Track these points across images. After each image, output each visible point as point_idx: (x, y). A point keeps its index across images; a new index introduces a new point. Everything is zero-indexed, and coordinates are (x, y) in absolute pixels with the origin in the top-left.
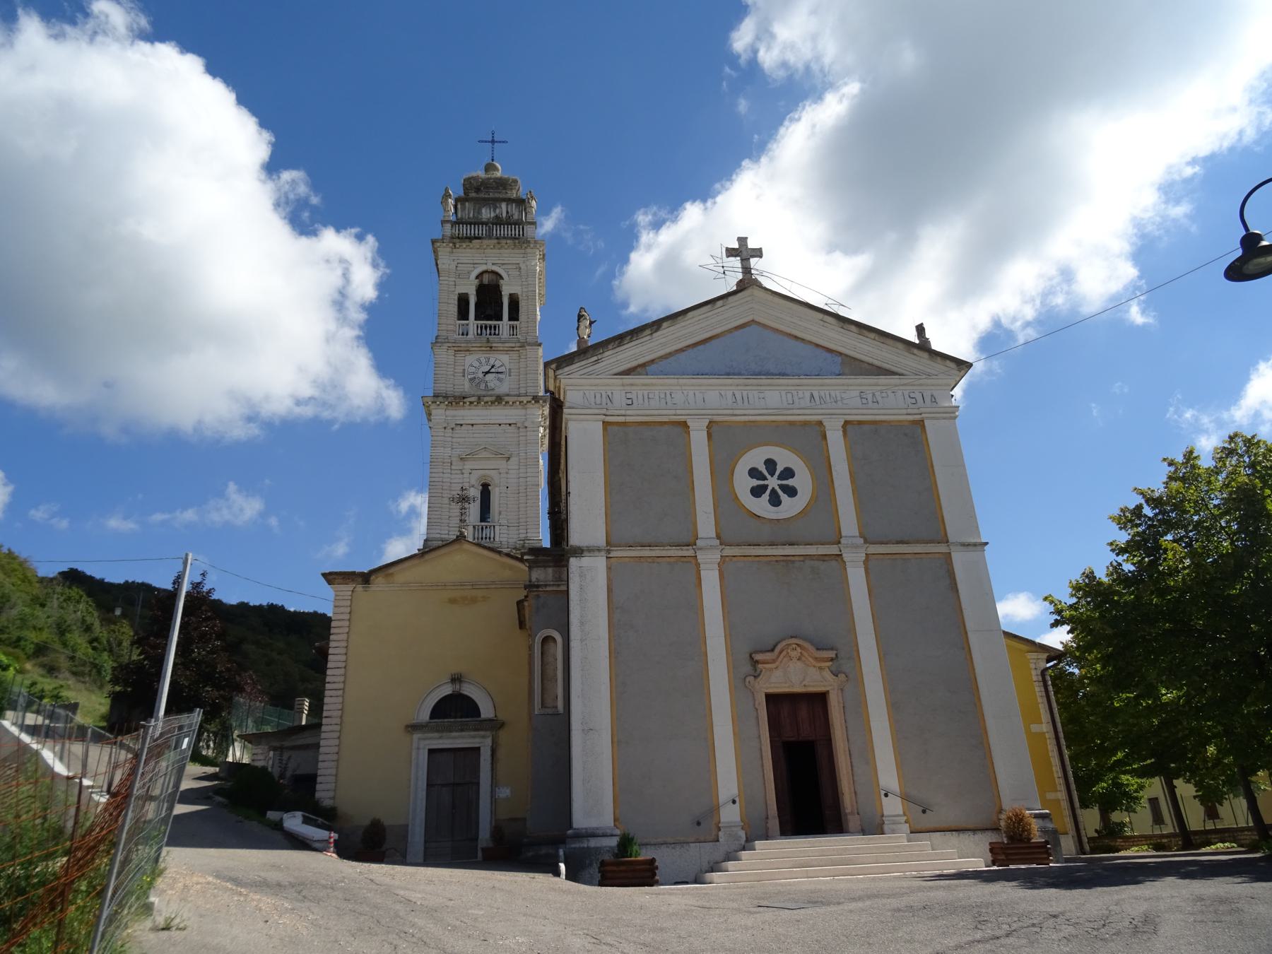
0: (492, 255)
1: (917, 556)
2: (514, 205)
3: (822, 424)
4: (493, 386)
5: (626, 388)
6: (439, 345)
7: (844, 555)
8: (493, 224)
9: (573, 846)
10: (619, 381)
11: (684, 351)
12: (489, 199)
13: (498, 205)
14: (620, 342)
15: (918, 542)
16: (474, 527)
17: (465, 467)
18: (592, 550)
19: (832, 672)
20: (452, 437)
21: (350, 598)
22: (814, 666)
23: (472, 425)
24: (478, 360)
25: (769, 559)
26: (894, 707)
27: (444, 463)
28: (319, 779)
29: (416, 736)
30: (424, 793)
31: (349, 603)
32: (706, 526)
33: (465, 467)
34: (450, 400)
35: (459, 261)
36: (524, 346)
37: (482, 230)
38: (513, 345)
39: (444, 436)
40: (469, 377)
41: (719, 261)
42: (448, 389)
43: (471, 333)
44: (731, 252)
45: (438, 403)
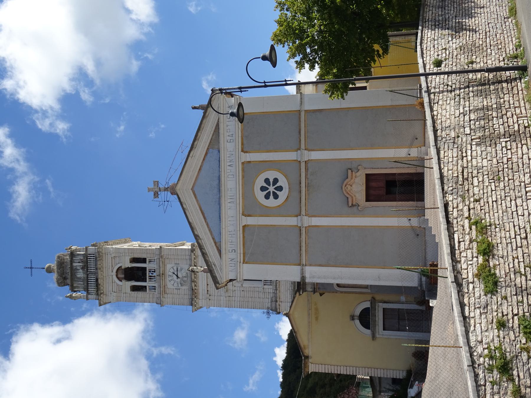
0: (107, 272)
1: (306, 125)
2: (74, 258)
3: (243, 162)
4: (185, 273)
5: (227, 252)
6: (162, 302)
7: (306, 160)
8: (88, 271)
9: (424, 287)
10: (224, 255)
11: (208, 223)
12: (71, 273)
13: (75, 268)
14: (205, 254)
15: (300, 125)
16: (264, 285)
17: (231, 289)
18: (302, 272)
19: (357, 172)
20: (215, 296)
21: (315, 365)
22: (355, 179)
23: (208, 285)
24: (170, 281)
25: (307, 194)
26: (372, 146)
27: (229, 301)
28: (395, 377)
29: (377, 336)
30: (402, 332)
31: (317, 365)
32: (292, 221)
33: (231, 289)
34: (194, 297)
35: (111, 291)
36: (162, 256)
37: (92, 278)
38: (161, 262)
39: (214, 300)
40: (180, 286)
41: (161, 203)
42: (187, 298)
43: (154, 285)
44: (156, 195)
45: (196, 303)
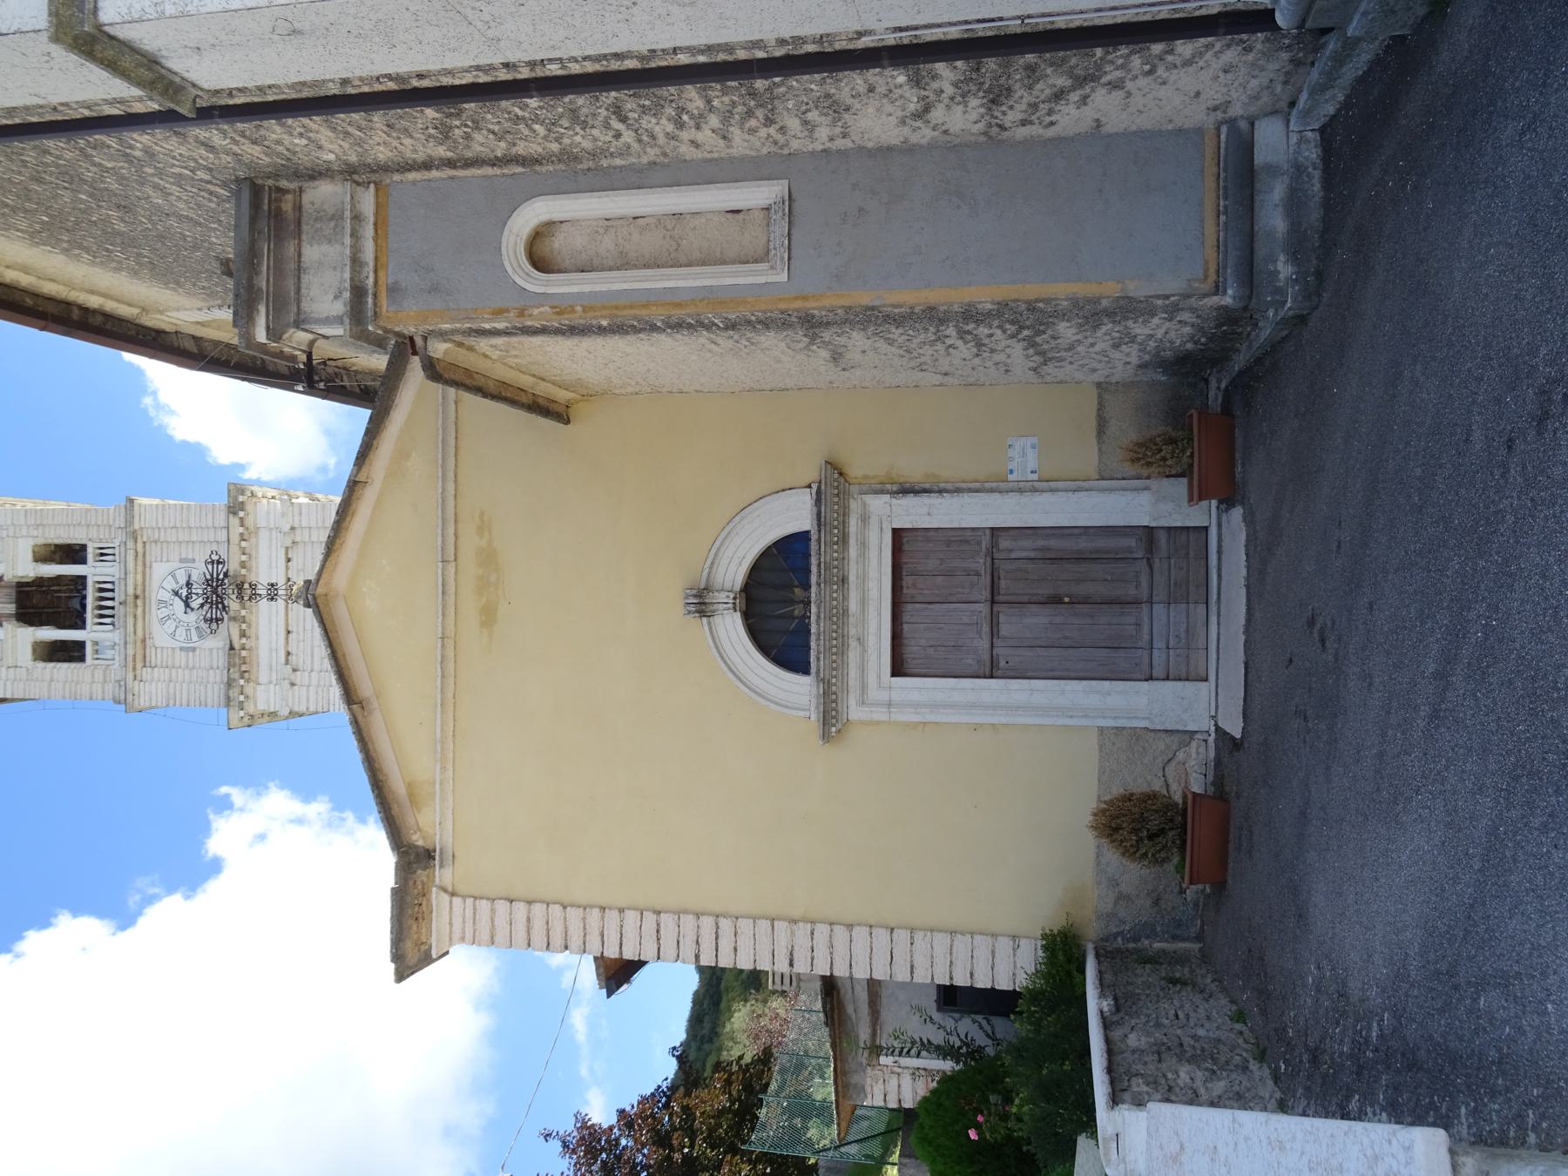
6: (130, 698)
23: (289, 632)
24: (163, 621)
29: (854, 711)
31: (484, 905)
34: (236, 676)
40: (195, 638)
42: (218, 679)
45: (242, 698)
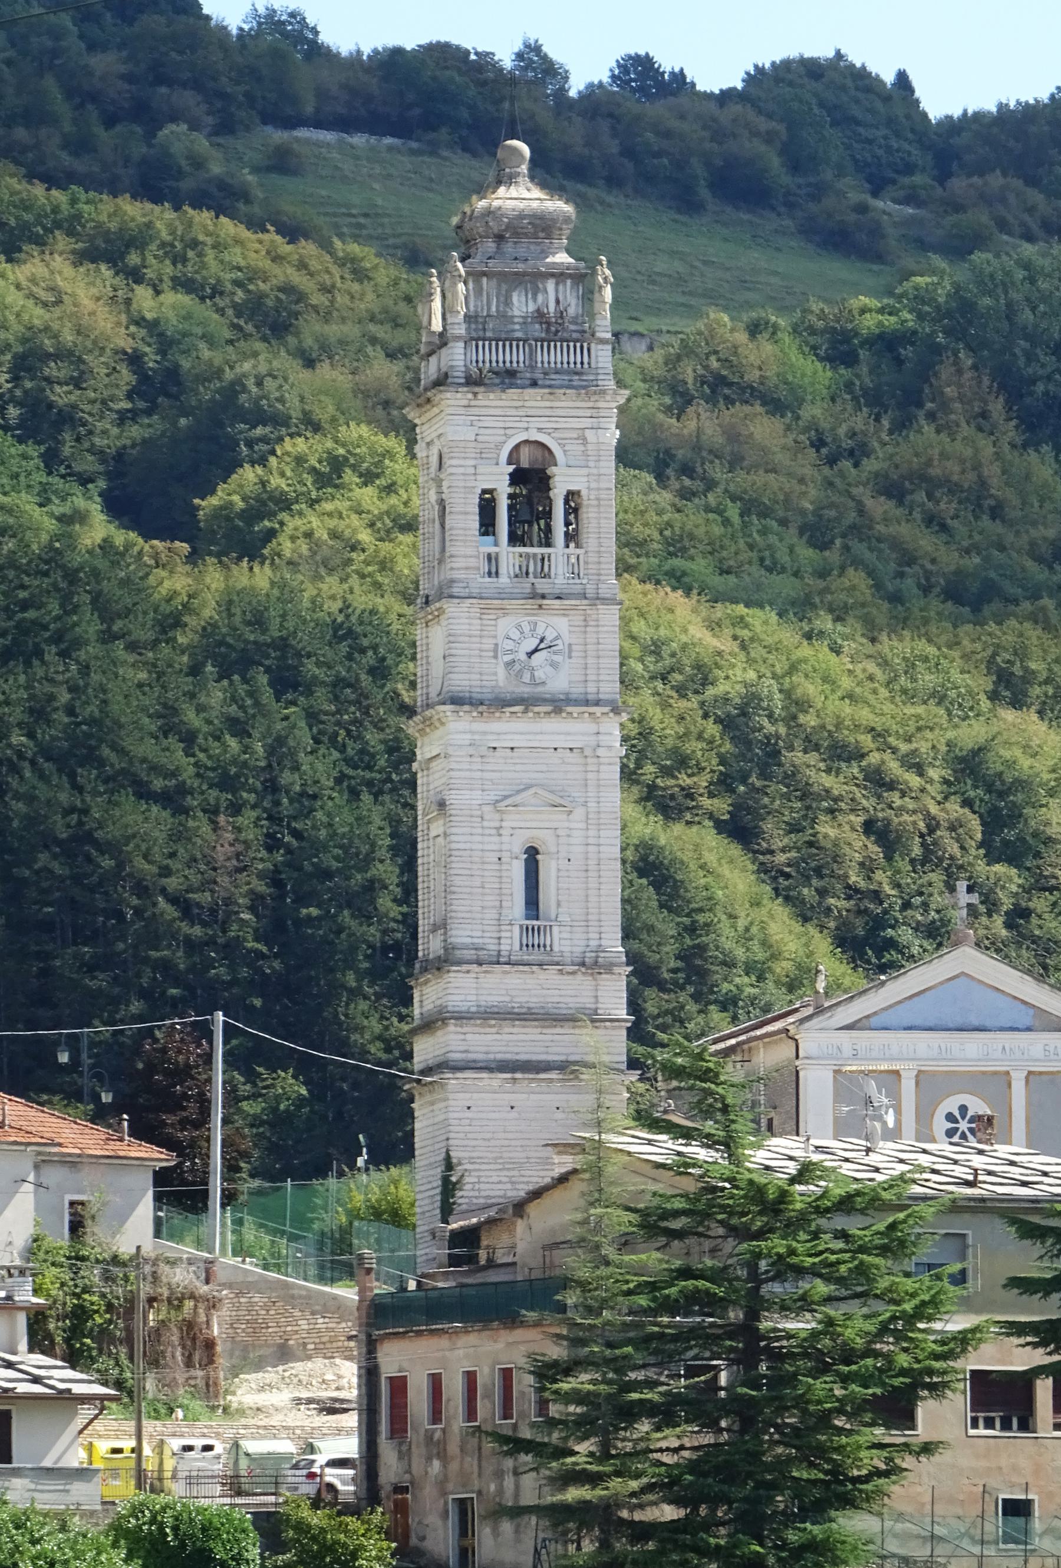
2: (569, 282)
8: (536, 341)
12: (524, 274)
17: (504, 824)
24: (519, 627)
33: (504, 824)
35: (481, 424)
42: (474, 683)
